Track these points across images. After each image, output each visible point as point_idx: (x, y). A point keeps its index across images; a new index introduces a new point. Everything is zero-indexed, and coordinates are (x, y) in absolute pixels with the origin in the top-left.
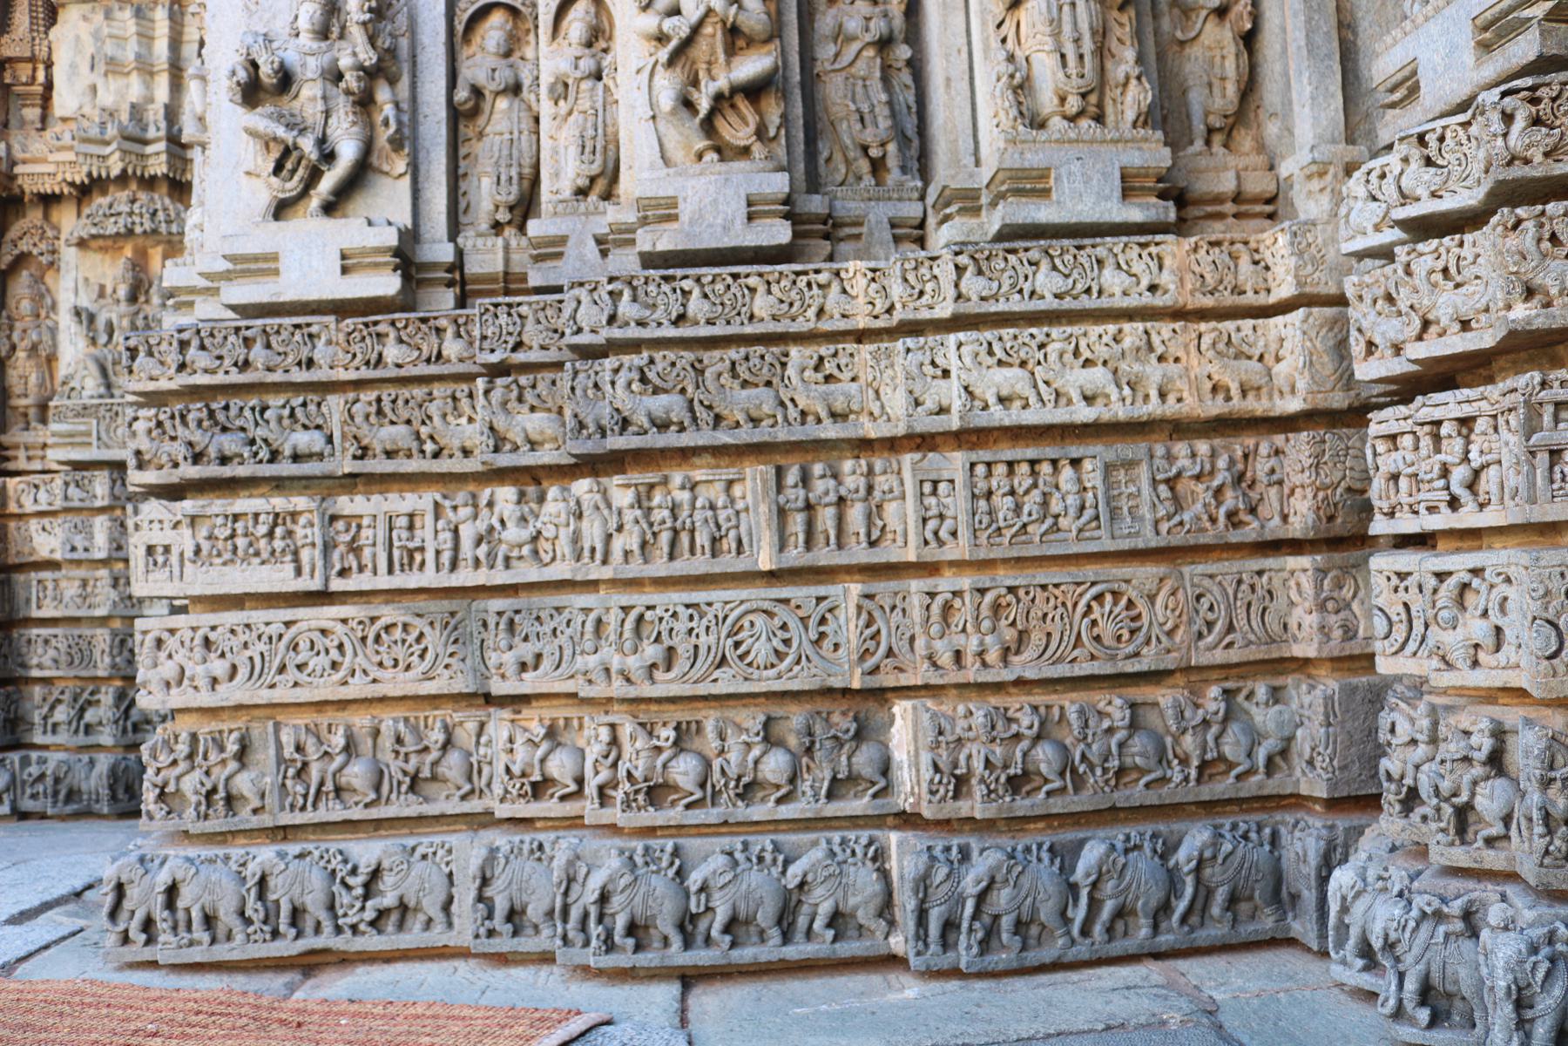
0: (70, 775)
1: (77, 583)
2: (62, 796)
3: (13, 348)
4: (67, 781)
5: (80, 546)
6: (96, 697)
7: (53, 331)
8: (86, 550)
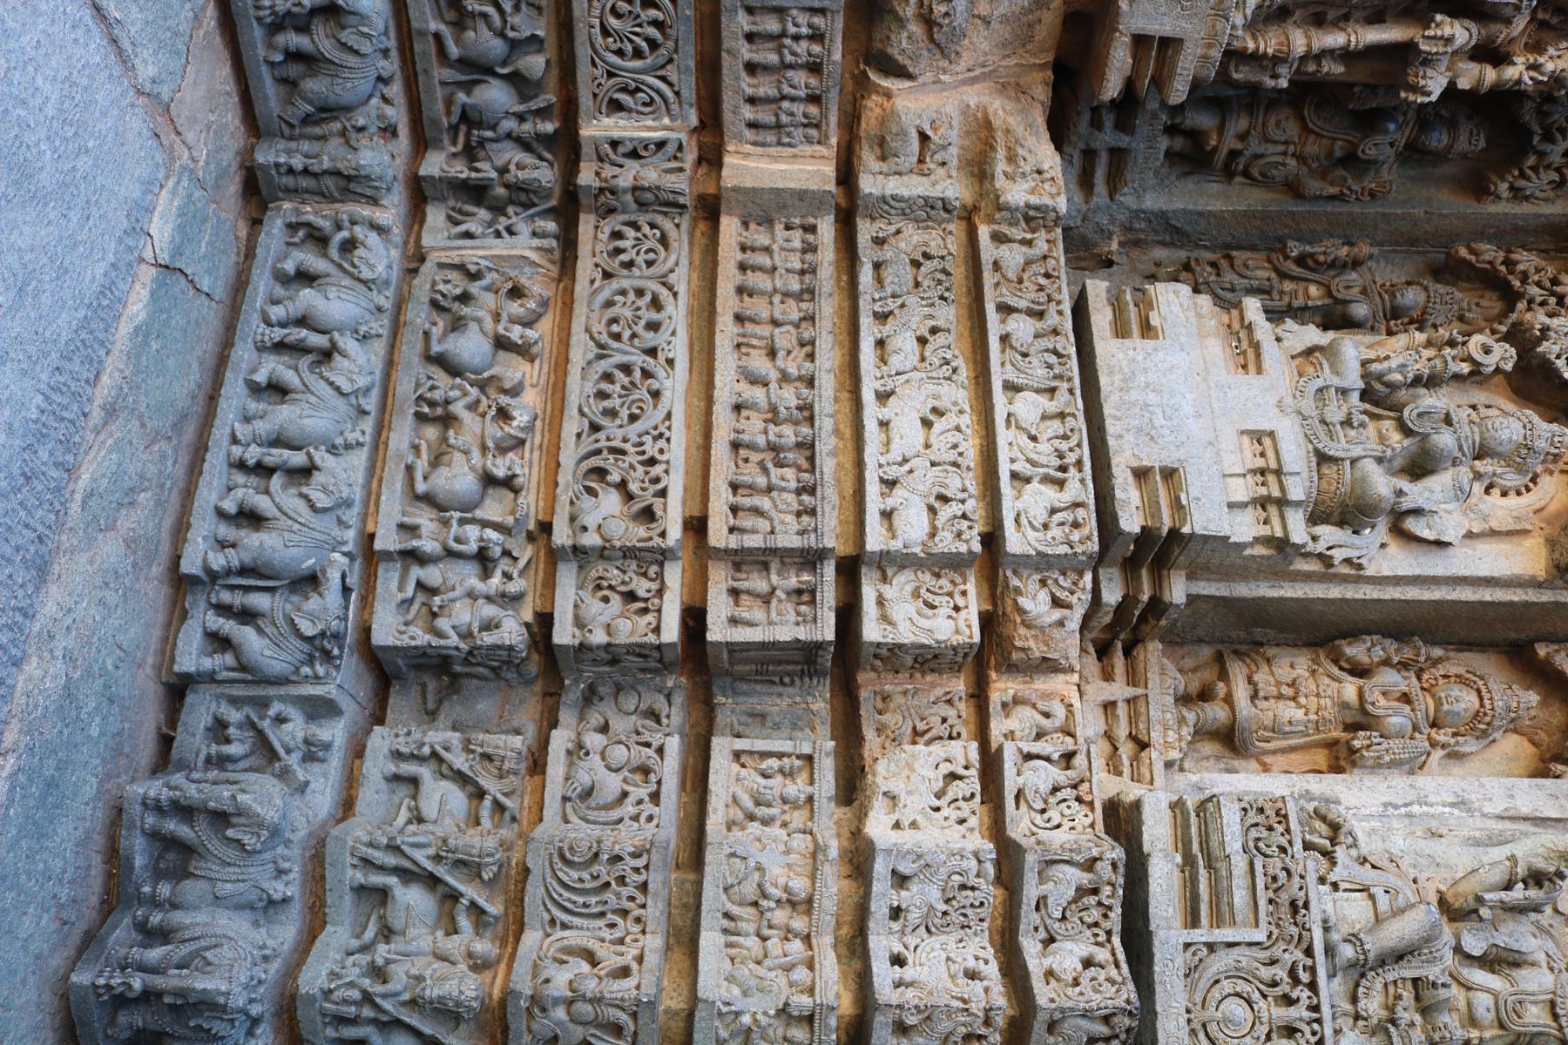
0: (231, 854)
1: (800, 885)
2: (172, 826)
4: (215, 846)
5: (903, 897)
6: (464, 922)
7: (1415, 766)
8: (896, 913)
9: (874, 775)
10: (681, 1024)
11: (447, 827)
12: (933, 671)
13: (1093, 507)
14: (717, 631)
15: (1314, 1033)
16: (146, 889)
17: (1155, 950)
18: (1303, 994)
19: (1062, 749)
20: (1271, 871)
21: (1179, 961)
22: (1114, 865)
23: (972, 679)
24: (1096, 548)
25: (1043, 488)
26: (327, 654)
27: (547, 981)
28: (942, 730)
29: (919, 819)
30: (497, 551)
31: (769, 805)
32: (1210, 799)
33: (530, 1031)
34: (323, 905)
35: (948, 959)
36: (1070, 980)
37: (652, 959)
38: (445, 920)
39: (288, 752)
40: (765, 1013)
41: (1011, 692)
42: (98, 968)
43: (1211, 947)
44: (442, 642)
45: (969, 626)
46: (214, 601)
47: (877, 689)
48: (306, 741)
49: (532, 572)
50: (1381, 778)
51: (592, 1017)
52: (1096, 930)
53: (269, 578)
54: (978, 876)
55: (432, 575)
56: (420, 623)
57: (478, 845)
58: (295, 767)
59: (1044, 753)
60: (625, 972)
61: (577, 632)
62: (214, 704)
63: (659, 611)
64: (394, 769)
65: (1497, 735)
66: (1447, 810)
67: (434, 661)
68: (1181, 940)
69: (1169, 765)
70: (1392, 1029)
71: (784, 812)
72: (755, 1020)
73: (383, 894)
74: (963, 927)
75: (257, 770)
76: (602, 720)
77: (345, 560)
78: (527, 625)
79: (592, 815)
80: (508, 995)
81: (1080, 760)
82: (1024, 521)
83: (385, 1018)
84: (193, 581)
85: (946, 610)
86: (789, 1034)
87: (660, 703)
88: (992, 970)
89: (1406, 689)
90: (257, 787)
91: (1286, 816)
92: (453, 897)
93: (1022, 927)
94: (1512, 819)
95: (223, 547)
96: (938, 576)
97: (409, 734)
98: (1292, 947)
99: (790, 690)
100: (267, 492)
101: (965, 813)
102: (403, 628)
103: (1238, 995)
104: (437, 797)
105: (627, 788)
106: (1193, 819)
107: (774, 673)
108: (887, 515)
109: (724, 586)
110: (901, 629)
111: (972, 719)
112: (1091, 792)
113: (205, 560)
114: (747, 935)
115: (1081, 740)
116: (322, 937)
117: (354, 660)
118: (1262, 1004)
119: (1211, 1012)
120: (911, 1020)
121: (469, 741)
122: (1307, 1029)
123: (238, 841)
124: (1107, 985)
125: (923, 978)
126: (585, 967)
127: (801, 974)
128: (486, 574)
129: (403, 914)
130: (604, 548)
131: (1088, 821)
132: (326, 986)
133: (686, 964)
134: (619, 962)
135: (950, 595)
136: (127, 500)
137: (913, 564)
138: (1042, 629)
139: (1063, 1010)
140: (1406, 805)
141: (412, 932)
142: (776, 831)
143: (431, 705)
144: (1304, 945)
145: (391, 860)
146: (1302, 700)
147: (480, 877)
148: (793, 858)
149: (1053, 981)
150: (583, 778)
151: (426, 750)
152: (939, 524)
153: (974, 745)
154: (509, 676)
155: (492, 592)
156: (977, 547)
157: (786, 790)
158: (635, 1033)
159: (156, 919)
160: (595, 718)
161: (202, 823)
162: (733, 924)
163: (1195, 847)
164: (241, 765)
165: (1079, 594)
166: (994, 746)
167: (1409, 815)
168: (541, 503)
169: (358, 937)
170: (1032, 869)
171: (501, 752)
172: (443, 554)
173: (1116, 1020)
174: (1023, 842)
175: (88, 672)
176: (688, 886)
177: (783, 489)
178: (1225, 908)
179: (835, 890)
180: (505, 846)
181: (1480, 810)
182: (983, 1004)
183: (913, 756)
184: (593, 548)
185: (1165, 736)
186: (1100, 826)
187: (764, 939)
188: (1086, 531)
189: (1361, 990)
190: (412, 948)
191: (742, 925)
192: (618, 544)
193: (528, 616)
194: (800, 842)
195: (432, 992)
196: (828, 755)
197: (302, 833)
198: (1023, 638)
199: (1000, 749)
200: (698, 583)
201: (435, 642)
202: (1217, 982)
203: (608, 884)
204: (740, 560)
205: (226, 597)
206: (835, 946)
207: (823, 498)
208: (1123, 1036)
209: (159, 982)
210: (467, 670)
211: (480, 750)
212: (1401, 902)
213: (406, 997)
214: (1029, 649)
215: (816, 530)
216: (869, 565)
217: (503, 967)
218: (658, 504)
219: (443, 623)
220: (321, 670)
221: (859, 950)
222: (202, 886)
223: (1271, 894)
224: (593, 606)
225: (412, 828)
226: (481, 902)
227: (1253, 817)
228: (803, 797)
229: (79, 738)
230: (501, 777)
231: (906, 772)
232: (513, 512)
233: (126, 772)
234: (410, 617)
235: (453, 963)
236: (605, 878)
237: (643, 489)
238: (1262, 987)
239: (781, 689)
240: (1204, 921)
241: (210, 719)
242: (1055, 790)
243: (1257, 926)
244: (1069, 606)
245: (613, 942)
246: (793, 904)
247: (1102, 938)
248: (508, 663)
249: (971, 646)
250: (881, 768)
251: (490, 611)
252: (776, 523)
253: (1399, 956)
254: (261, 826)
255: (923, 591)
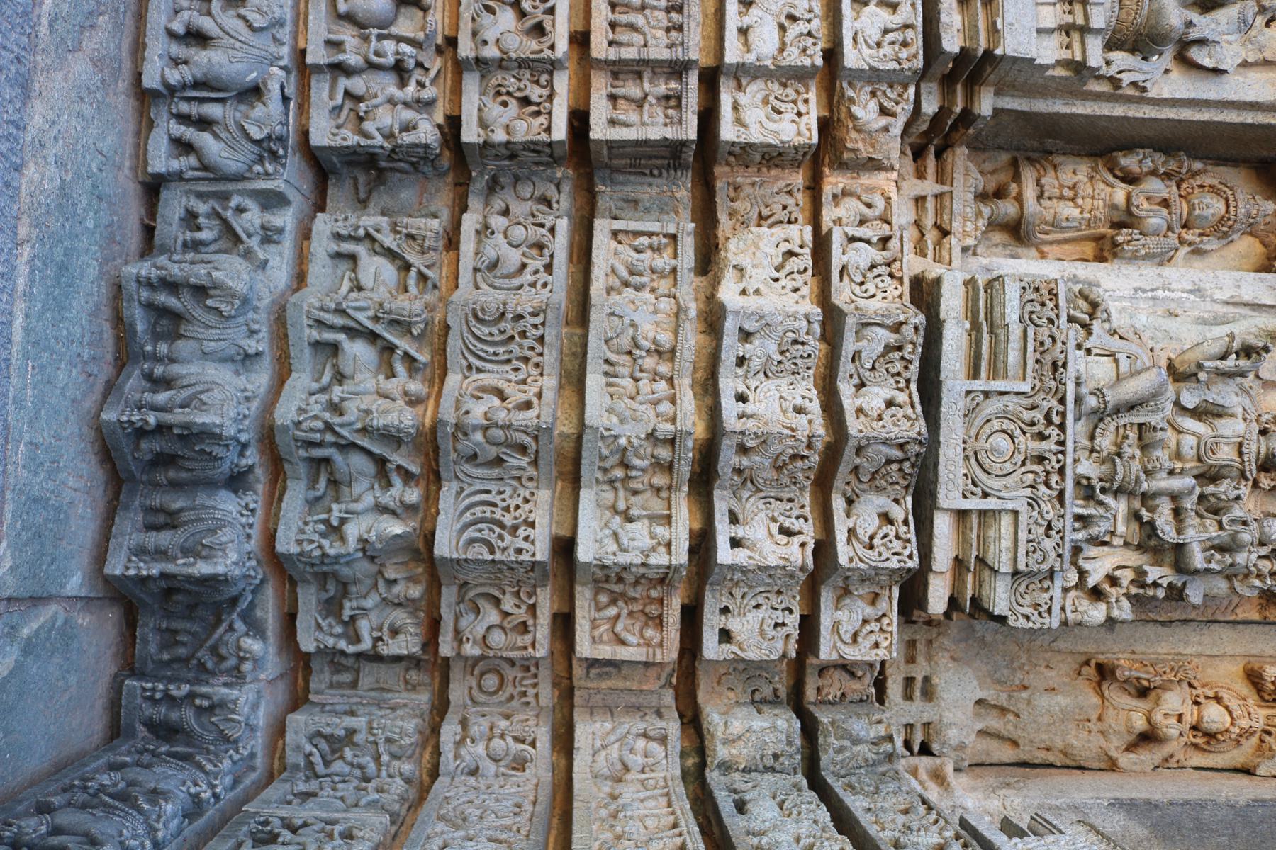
0: (212, 319)
1: (665, 338)
2: (162, 298)
3: (1130, 179)
4: (198, 313)
5: (748, 349)
6: (400, 368)
7: (1164, 259)
8: (741, 361)
9: (726, 251)
10: (572, 445)
11: (381, 294)
12: (777, 166)
13: (920, 29)
14: (599, 131)
15: (1058, 461)
16: (149, 348)
17: (943, 395)
18: (1054, 432)
19: (880, 234)
20: (1040, 338)
21: (961, 404)
22: (916, 329)
23: (809, 173)
24: (921, 65)
25: (878, 10)
26: (274, 155)
27: (467, 412)
28: (783, 216)
29: (762, 287)
30: (411, 63)
31: (640, 275)
32: (997, 279)
33: (455, 450)
34: (288, 357)
35: (781, 397)
36: (876, 415)
37: (549, 395)
38: (384, 366)
39: (249, 236)
40: (637, 437)
41: (841, 186)
42: (120, 408)
43: (987, 394)
44: (369, 142)
45: (809, 130)
46: (174, 111)
47: (730, 180)
48: (263, 227)
49: (441, 81)
50: (1136, 267)
51: (503, 439)
52: (898, 379)
53: (219, 90)
54: (807, 333)
55: (357, 84)
56: (350, 126)
57: (408, 308)
58: (256, 248)
59: (865, 237)
60: (527, 405)
61: (482, 132)
62: (184, 199)
63: (550, 113)
64: (336, 248)
65: (1235, 237)
66: (1185, 295)
67: (363, 158)
68: (964, 389)
69: (965, 250)
70: (1118, 460)
71: (653, 280)
72: (630, 442)
73: (335, 348)
74: (794, 373)
75: (226, 252)
76: (503, 205)
77: (282, 73)
78: (439, 126)
79: (498, 283)
80: (437, 424)
81: (894, 244)
82: (860, 39)
83: (343, 442)
84: (154, 94)
85: (790, 115)
86: (656, 453)
87: (551, 191)
88: (815, 407)
89: (1166, 196)
90: (227, 266)
91: (1056, 295)
92: (390, 349)
93: (840, 374)
94: (1235, 304)
95: (177, 65)
96: (785, 86)
97: (346, 219)
98: (1049, 397)
99: (658, 181)
100: (209, 14)
101: (799, 284)
102: (336, 131)
103: (1004, 431)
104: (372, 270)
105: (525, 260)
106: (982, 294)
107: (645, 166)
108: (744, 32)
109: (604, 93)
110: (752, 131)
111: (808, 207)
112: (901, 270)
113: (163, 76)
114: (623, 377)
115: (896, 227)
116: (290, 381)
117: (297, 158)
118: (1021, 439)
119: (982, 443)
120: (751, 443)
121: (396, 224)
122: (1053, 458)
123: (217, 309)
124: (903, 420)
125: (760, 412)
126: (496, 402)
127: (665, 407)
128: (403, 84)
129: (351, 362)
130: (502, 59)
131: (897, 293)
132: (296, 419)
133: (575, 399)
134: (523, 397)
135: (795, 102)
136: (88, 23)
137: (764, 75)
138: (870, 133)
139: (868, 439)
140: (1152, 290)
141: (359, 377)
142: (646, 295)
143: (362, 195)
144: (1059, 396)
145: (339, 321)
146: (1080, 201)
147: (411, 333)
148: (660, 317)
149: (862, 417)
150: (490, 253)
151: (361, 232)
152: (788, 41)
153: (809, 229)
154: (426, 169)
155: (409, 99)
156: (819, 61)
157: (654, 263)
158: (537, 451)
159: (159, 370)
160: (498, 204)
161: (186, 296)
162: (612, 368)
163: (982, 317)
164: (212, 248)
165: (903, 105)
166: (825, 230)
167: (1154, 298)
168: (447, 20)
169: (317, 381)
170: (851, 330)
171: (423, 233)
172: (365, 66)
173: (909, 447)
174: (845, 308)
175: (78, 175)
176: (576, 339)
177: (655, 8)
178: (1001, 365)
179: (693, 342)
180: (429, 308)
181: (1211, 296)
182: (807, 432)
183: (759, 236)
184: (493, 60)
185: (964, 226)
186: (907, 297)
187: (637, 380)
188: (913, 50)
189: (1098, 430)
190: (361, 388)
191: (619, 369)
192: (514, 56)
193: (440, 119)
194: (666, 305)
195: (378, 421)
196: (689, 234)
197: (266, 301)
198: (855, 141)
199: (830, 232)
200: (583, 89)
201: (364, 142)
202: (989, 421)
203: (512, 338)
204: (618, 70)
205: (184, 107)
206: (692, 387)
207: (689, 16)
208: (913, 459)
209: (168, 418)
210: (391, 165)
211: (404, 231)
212: (1139, 365)
213: (359, 425)
214: (858, 150)
215: (682, 44)
216: (727, 75)
217: (431, 403)
218: (547, 20)
219: (369, 126)
220: (270, 168)
221: (711, 389)
222: (192, 345)
223: (1038, 355)
224: (494, 110)
225: (354, 295)
226: (412, 352)
227: (1030, 295)
228: (668, 268)
229: (78, 230)
230: (423, 253)
231: (753, 249)
232: (423, 29)
233: (120, 257)
234: (341, 121)
235: (393, 400)
236: (510, 333)
237: (534, 7)
238: (1023, 426)
239: (650, 180)
240: (983, 374)
241: (182, 211)
242: (873, 267)
243: (1024, 379)
244: (894, 115)
245: (518, 383)
246: (659, 353)
247: (902, 385)
248: (425, 158)
249: (810, 146)
250: (732, 245)
251: (407, 115)
252: (649, 37)
253: (1131, 407)
254: (233, 296)
255: (772, 98)
